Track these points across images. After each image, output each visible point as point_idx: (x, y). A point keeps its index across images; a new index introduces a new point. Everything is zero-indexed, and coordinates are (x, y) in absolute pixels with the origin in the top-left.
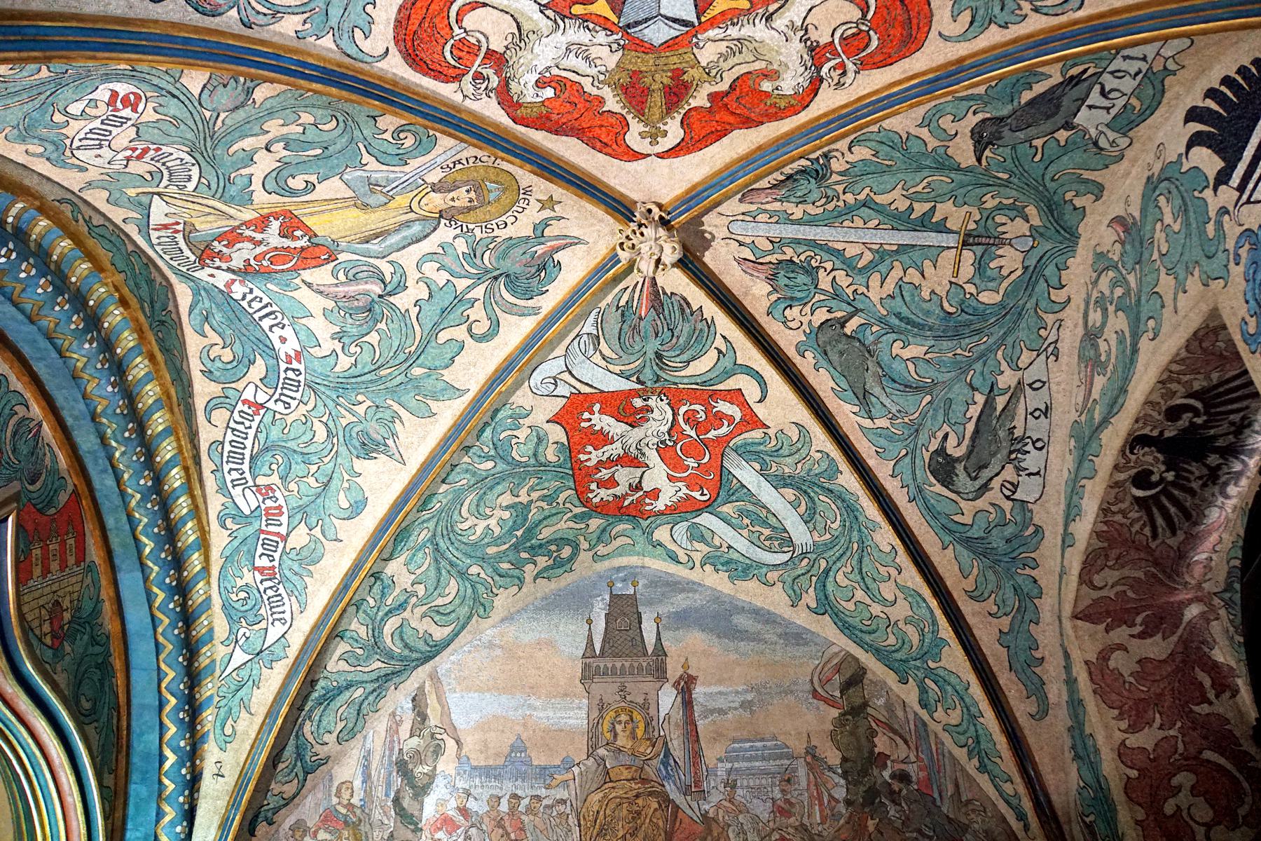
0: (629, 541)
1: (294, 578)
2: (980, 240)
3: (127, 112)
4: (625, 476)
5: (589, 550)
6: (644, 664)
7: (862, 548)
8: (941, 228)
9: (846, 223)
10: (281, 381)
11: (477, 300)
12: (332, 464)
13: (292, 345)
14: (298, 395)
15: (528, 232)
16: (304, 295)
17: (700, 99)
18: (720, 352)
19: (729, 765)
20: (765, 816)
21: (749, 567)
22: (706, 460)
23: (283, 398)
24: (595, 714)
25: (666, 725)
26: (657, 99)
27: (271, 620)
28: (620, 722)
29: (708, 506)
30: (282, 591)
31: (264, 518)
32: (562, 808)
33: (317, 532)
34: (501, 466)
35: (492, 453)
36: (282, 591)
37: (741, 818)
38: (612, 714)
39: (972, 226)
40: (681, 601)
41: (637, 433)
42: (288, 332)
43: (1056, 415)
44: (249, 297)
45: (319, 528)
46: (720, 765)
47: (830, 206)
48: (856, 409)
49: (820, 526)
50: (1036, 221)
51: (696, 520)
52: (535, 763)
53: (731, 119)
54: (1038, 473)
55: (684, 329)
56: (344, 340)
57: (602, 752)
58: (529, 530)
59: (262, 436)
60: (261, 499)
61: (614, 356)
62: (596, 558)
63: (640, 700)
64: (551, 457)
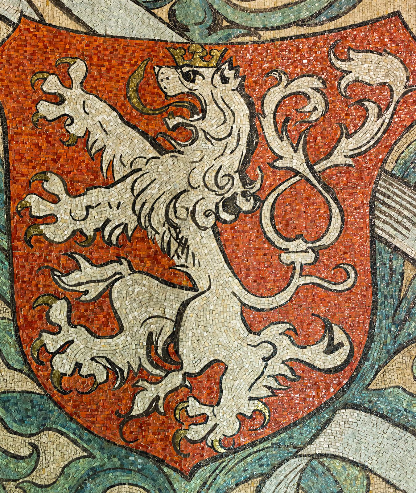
4: (137, 298)
29: (347, 388)
41: (166, 174)
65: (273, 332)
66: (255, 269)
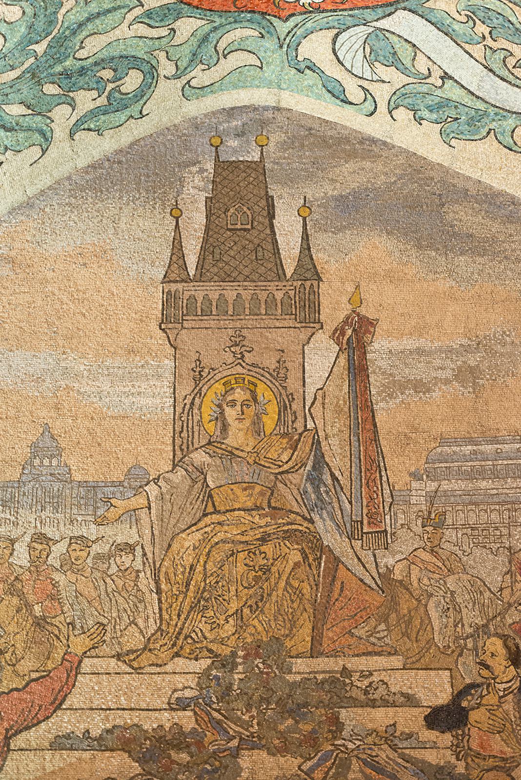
0: (252, 60)
5: (177, 77)
6: (279, 295)
19: (432, 486)
20: (495, 580)
24: (186, 389)
25: (317, 410)
28: (233, 404)
32: (127, 560)
37: (451, 582)
38: (219, 388)
40: (350, 176)
46: (415, 485)
51: (384, 24)
52: (77, 477)
57: (199, 457)
58: (60, 42)
62: (189, 91)
63: (271, 362)
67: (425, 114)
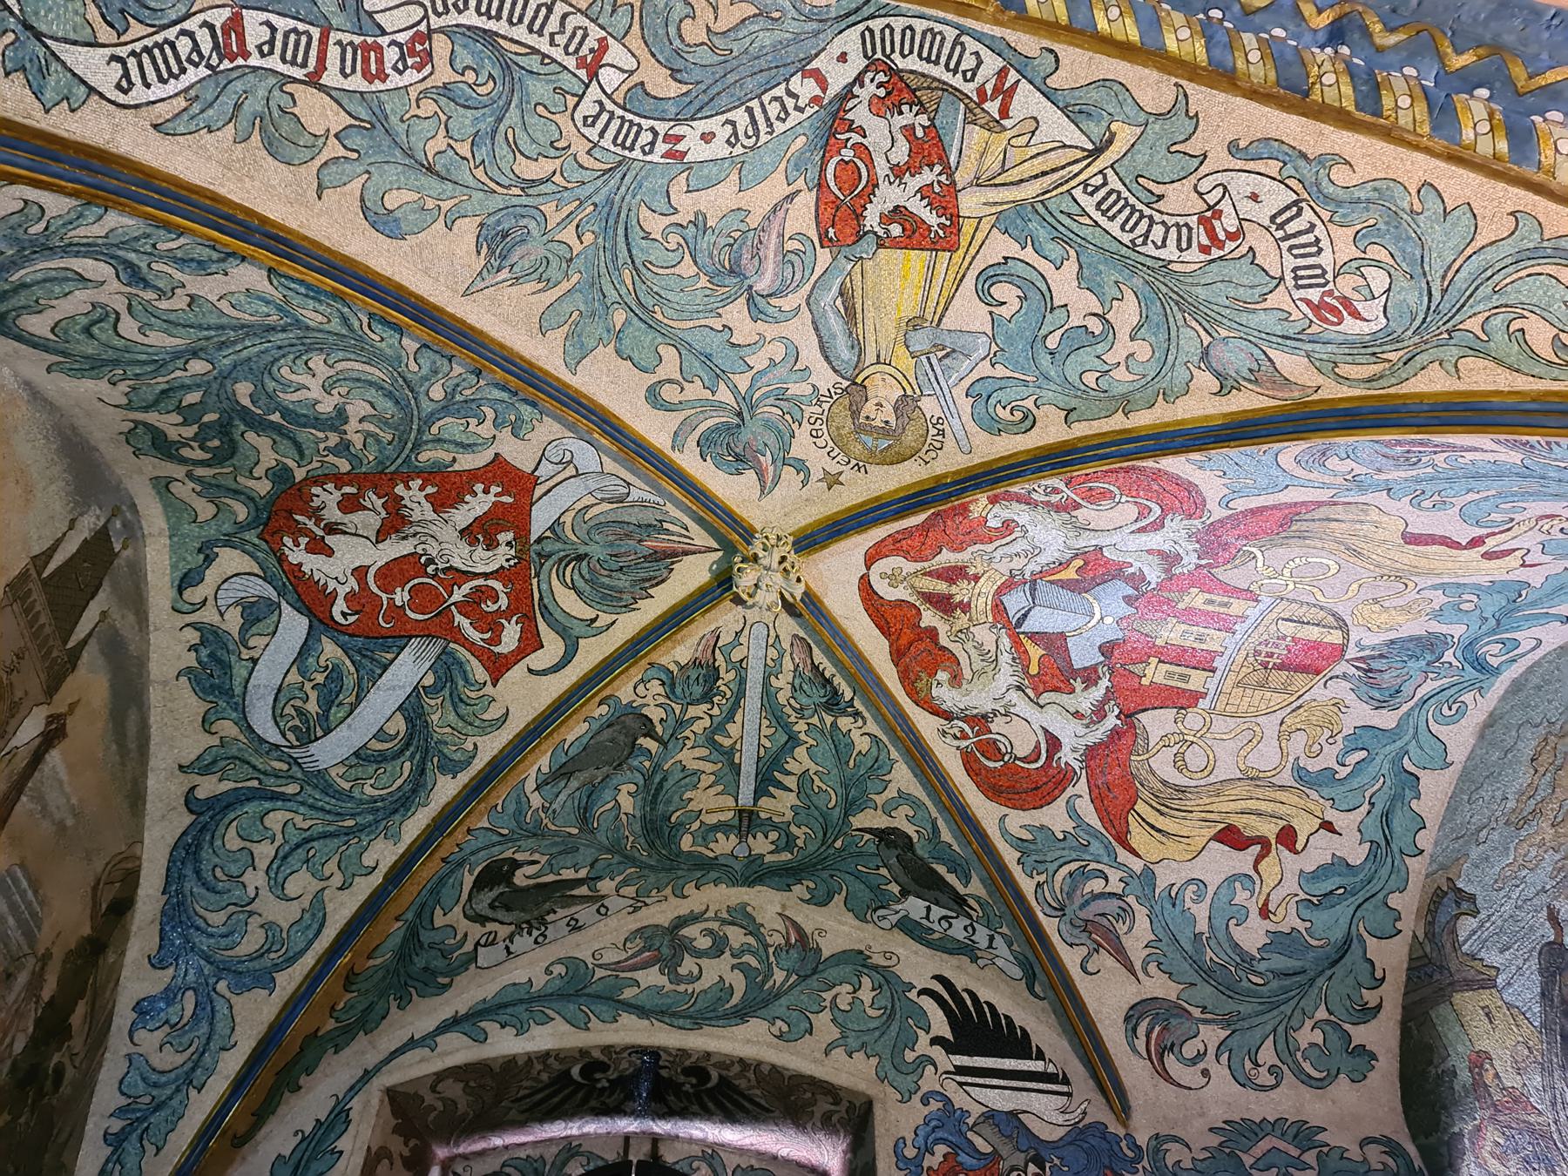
1: (228, 101)
2: (747, 821)
3: (1314, 295)
4: (368, 520)
7: (349, 832)
8: (759, 793)
9: (765, 723)
10: (637, 120)
11: (713, 393)
12: (471, 182)
13: (696, 150)
14: (606, 143)
15: (796, 451)
16: (776, 187)
17: (929, 618)
18: (593, 621)
21: (228, 693)
22: (412, 615)
23: (605, 116)
26: (941, 587)
27: (122, 52)
30: (193, 74)
31: (357, 40)
33: (334, 149)
34: (427, 407)
35: (458, 398)
36: (193, 74)
39: (762, 815)
41: (448, 534)
42: (719, 149)
43: (577, 936)
44: (790, 103)
45: (342, 152)
47: (788, 710)
48: (545, 769)
49: (359, 772)
50: (768, 859)
53: (903, 641)
54: (509, 953)
55: (622, 581)
56: (692, 228)
59: (533, 63)
60: (402, 38)
61: (587, 517)
64: (423, 457)
65: (353, 583)
66: (392, 574)
67: (204, 652)
